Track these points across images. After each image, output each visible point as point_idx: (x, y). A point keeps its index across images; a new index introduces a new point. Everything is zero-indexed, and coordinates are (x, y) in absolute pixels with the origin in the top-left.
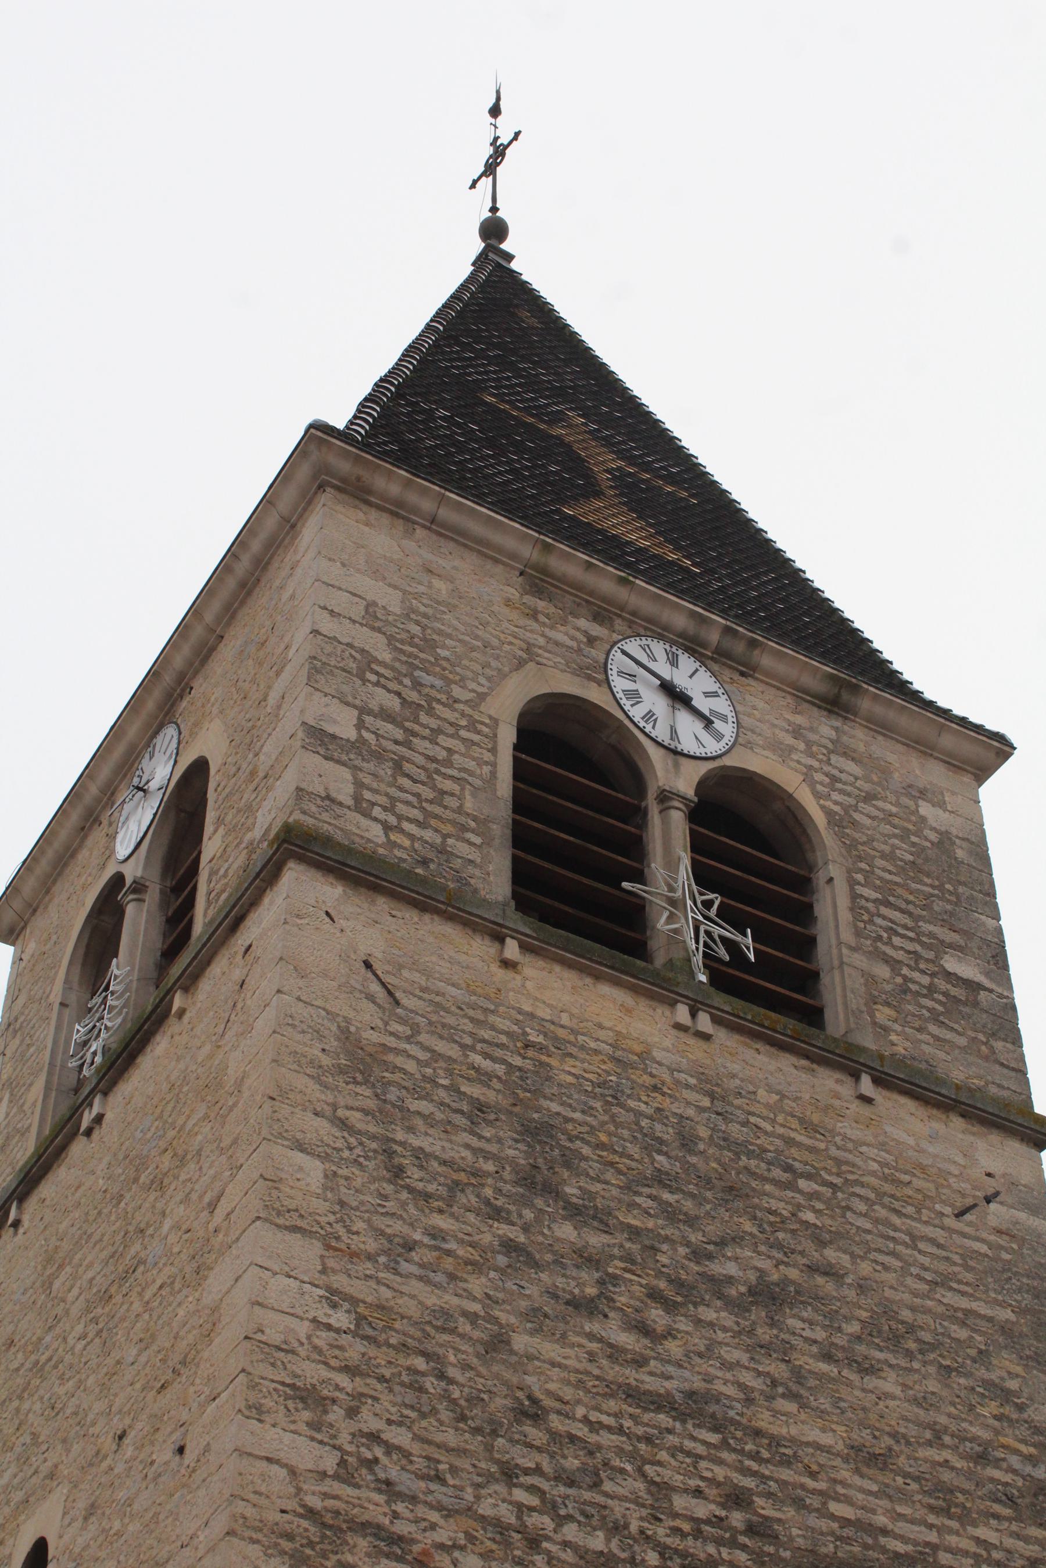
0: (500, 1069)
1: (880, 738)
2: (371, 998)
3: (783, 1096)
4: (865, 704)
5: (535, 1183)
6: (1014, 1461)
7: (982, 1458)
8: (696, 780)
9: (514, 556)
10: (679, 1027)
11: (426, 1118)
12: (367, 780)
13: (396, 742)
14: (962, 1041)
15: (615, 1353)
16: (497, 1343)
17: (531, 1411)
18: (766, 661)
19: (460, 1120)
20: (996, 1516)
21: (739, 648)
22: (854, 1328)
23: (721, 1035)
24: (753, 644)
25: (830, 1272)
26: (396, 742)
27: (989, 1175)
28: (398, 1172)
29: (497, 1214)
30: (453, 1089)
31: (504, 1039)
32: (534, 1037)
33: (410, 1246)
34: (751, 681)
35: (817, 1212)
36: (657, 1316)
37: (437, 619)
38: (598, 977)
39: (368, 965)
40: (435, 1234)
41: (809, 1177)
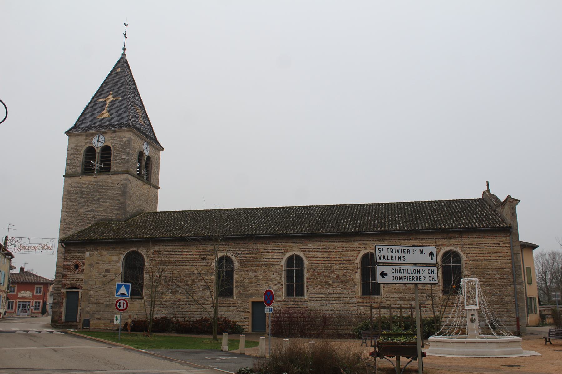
5: (81, 197)
16: (77, 211)
17: (79, 215)
25: (105, 195)
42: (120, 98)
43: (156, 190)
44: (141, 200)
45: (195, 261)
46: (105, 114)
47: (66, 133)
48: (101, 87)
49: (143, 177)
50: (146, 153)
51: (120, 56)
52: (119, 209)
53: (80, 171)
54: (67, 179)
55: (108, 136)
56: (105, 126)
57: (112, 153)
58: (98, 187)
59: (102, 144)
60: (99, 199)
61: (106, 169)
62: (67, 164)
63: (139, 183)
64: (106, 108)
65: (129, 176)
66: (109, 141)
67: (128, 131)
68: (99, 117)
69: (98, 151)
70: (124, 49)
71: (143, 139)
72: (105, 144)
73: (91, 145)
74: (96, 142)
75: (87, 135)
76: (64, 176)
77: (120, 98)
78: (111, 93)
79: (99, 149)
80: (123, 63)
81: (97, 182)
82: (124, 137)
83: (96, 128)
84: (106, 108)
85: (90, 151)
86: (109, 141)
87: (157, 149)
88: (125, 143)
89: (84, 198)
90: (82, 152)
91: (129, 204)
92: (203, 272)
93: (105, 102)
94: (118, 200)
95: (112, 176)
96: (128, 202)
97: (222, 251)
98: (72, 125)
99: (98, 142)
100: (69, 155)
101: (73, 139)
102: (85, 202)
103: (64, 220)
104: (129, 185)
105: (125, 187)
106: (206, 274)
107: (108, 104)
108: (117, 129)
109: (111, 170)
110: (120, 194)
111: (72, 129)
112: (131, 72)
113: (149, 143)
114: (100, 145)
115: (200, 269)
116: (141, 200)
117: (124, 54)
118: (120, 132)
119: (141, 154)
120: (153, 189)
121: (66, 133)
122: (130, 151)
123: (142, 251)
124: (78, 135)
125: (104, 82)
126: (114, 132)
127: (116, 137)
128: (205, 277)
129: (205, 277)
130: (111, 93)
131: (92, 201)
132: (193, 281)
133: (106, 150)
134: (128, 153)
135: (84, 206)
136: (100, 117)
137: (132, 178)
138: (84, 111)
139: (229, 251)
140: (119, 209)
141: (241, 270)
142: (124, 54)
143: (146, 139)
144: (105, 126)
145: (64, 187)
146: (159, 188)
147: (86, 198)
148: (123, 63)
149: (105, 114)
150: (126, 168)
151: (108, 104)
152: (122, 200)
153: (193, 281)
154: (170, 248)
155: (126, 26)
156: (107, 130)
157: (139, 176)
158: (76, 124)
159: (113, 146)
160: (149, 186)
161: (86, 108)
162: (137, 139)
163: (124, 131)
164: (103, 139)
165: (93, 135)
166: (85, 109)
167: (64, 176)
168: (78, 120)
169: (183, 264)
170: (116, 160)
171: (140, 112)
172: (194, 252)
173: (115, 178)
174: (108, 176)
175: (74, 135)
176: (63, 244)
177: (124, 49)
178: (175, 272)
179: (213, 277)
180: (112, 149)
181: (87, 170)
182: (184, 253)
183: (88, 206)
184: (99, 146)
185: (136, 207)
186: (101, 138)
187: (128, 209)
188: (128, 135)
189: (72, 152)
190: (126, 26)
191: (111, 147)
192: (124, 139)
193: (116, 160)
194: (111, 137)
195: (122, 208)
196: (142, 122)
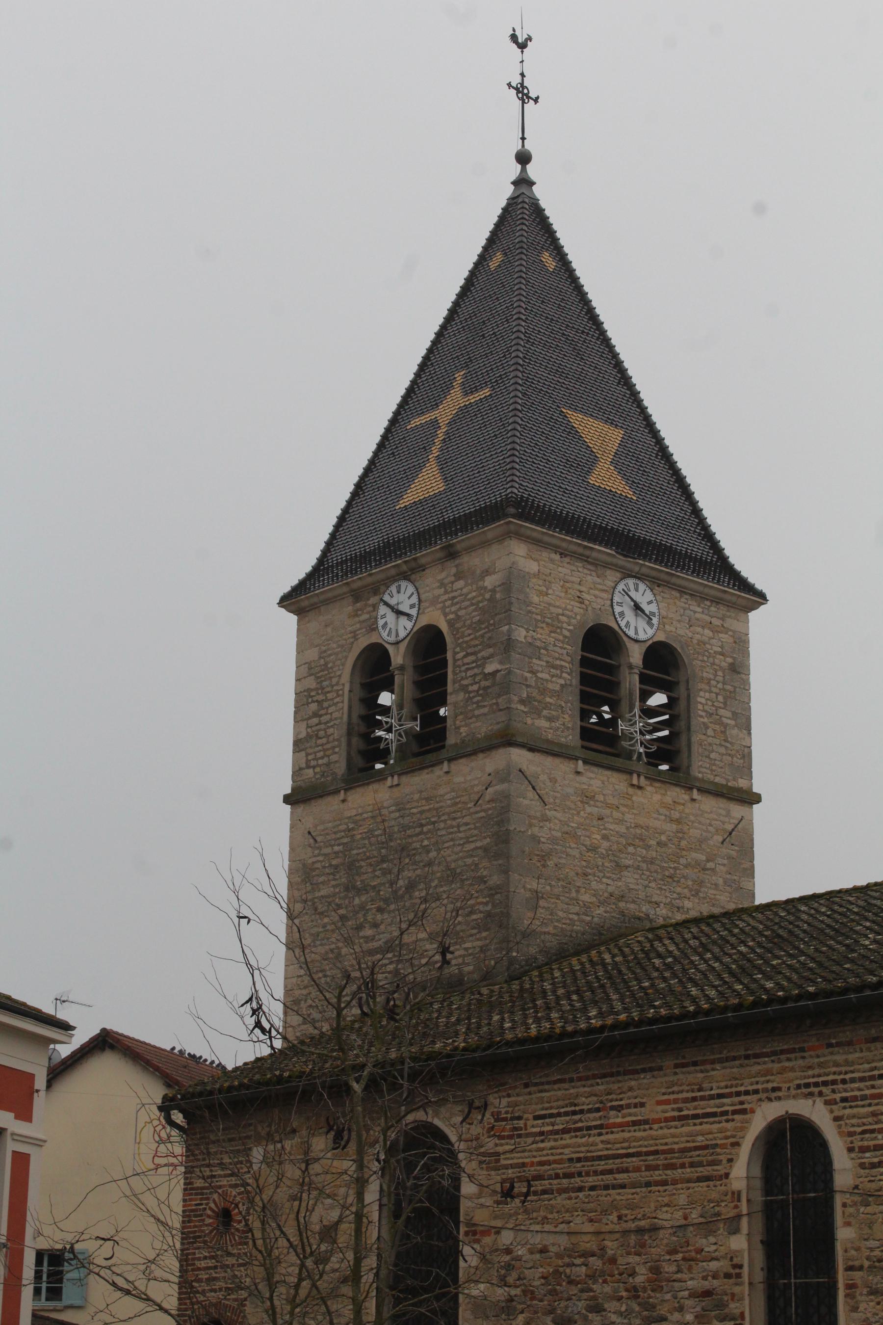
0: (341, 848)
1: (473, 554)
2: (310, 846)
3: (421, 792)
4: (459, 547)
6: (481, 908)
7: (471, 913)
8: (435, 623)
9: (345, 593)
10: (391, 787)
11: (323, 883)
12: (310, 751)
13: (317, 725)
14: (486, 710)
15: (367, 939)
18: (423, 561)
19: (331, 877)
20: (472, 935)
21: (413, 564)
22: (436, 882)
23: (404, 779)
24: (415, 559)
25: (430, 864)
26: (317, 725)
27: (489, 775)
28: (316, 909)
29: (339, 907)
30: (331, 865)
31: (343, 834)
32: (351, 826)
33: (318, 934)
34: (427, 571)
35: (427, 838)
36: (379, 917)
37: (329, 649)
38: (368, 784)
39: (309, 833)
40: (324, 926)
41: (427, 824)
42: (486, 392)
43: (737, 810)
44: (619, 867)
45: (661, 1160)
46: (428, 483)
47: (288, 601)
48: (426, 358)
49: (629, 755)
50: (639, 631)
51: (509, 190)
52: (482, 927)
53: (341, 768)
54: (300, 809)
55: (432, 579)
56: (423, 538)
57: (449, 655)
58: (404, 828)
59: (409, 625)
60: (411, 886)
61: (429, 743)
62: (298, 745)
63: (603, 782)
64: (435, 451)
65: (519, 756)
66: (434, 601)
67: (501, 539)
68: (408, 499)
69: (397, 658)
70: (523, 158)
71: (606, 565)
72: (424, 621)
73: (374, 639)
74: (391, 617)
75: (357, 596)
76: (287, 799)
77: (486, 392)
78: (459, 377)
79: (403, 647)
80: (524, 227)
81: (400, 806)
82: (487, 572)
83: (389, 550)
84: (435, 451)
85: (375, 667)
86: (434, 601)
87: (717, 601)
88: (492, 600)
89: (359, 892)
90: (344, 674)
91: (537, 896)
92: (694, 1216)
93: (434, 424)
94: (482, 880)
95: (455, 766)
96: (524, 885)
97: (773, 1094)
98: (309, 569)
99: (399, 615)
100: (303, 699)
101: (314, 625)
102: (362, 907)
103: (297, 1002)
104: (528, 801)
105: (503, 809)
106: (708, 1226)
107: (441, 434)
108: (460, 540)
109: (451, 739)
110: (486, 849)
111: (310, 576)
112: (483, 258)
113: (654, 582)
114: (404, 627)
115: (682, 1199)
116: (619, 867)
117: (523, 182)
118: (470, 549)
119: (600, 642)
120: (708, 804)
121: (288, 601)
122: (520, 634)
123: (448, 1121)
124: (328, 602)
125: (440, 335)
126: (451, 554)
127: (459, 576)
128: (708, 1244)
129: (708, 1244)
130: (459, 377)
131: (386, 901)
132: (656, 1270)
133: (429, 645)
134: (509, 645)
135: (360, 927)
136: (408, 499)
137: (549, 761)
138: (359, 487)
139: (807, 1090)
140: (482, 927)
141: (866, 1197)
142: (523, 182)
143: (621, 560)
144: (423, 538)
145: (292, 849)
146: (757, 799)
147: (365, 889)
148: (524, 227)
149: (428, 483)
150: (502, 717)
151: (441, 434)
152: (495, 880)
153: (656, 1270)
154: (555, 1096)
155: (522, 46)
156: (424, 555)
157: (600, 743)
158: (325, 553)
159: (451, 624)
160: (684, 796)
161: (368, 471)
162: (565, 569)
163: (486, 544)
164: (414, 600)
165: (377, 589)
166: (363, 478)
167: (287, 799)
168: (333, 536)
169: (609, 1179)
170: (464, 688)
171: (602, 436)
172: (652, 1104)
173: (469, 774)
174: (438, 771)
175: (314, 607)
176: (178, 1117)
177: (523, 158)
178: (579, 1223)
179: (739, 1243)
180: (449, 639)
181: (367, 757)
182: (616, 1118)
183: (375, 925)
184: (402, 634)
185: (587, 906)
186: (404, 596)
187: (523, 918)
188: (518, 556)
189: (311, 683)
190: (522, 46)
191: (444, 627)
192: (489, 582)
193: (464, 688)
194: (442, 585)
195: (499, 919)
196: (620, 486)
